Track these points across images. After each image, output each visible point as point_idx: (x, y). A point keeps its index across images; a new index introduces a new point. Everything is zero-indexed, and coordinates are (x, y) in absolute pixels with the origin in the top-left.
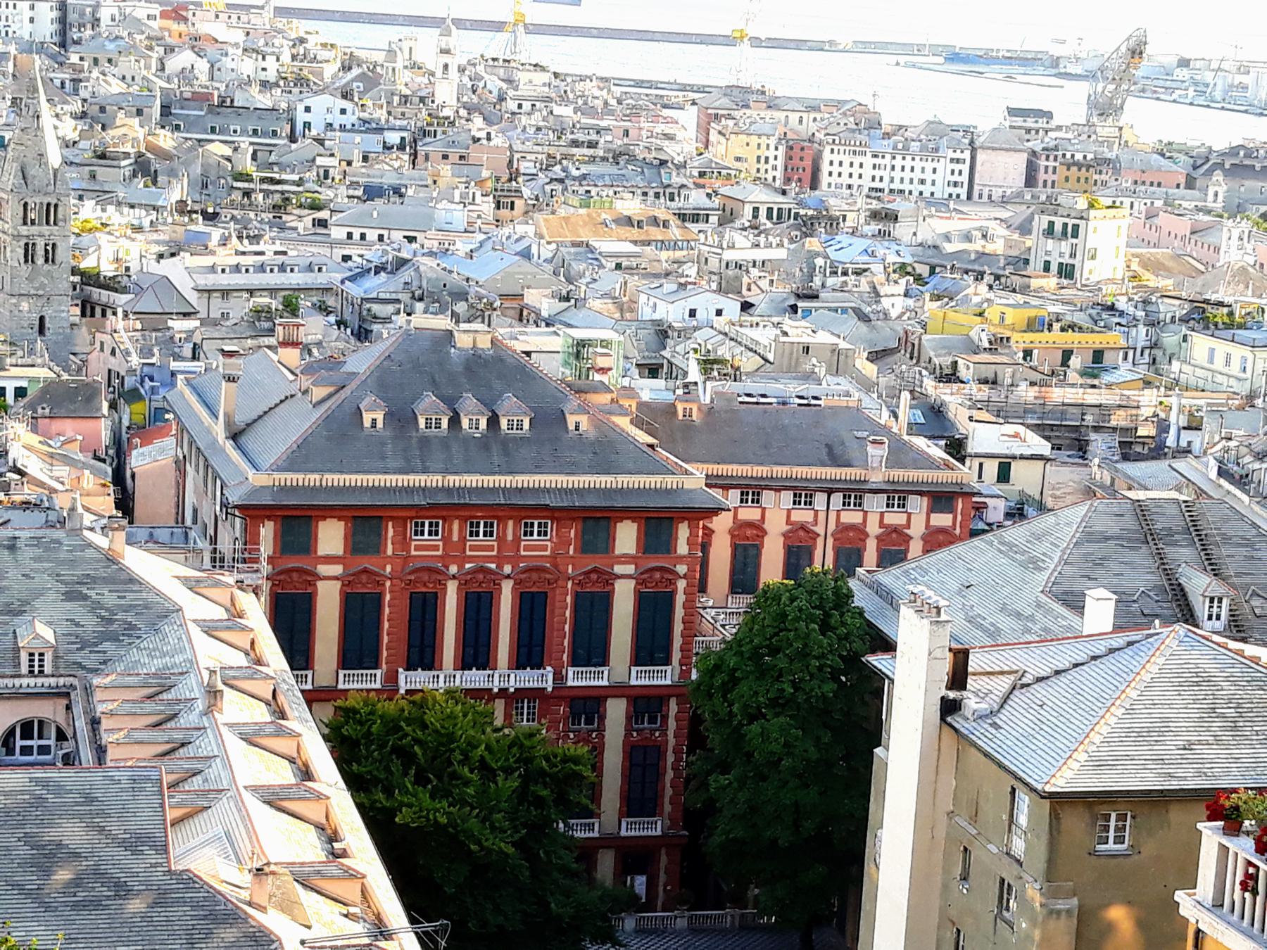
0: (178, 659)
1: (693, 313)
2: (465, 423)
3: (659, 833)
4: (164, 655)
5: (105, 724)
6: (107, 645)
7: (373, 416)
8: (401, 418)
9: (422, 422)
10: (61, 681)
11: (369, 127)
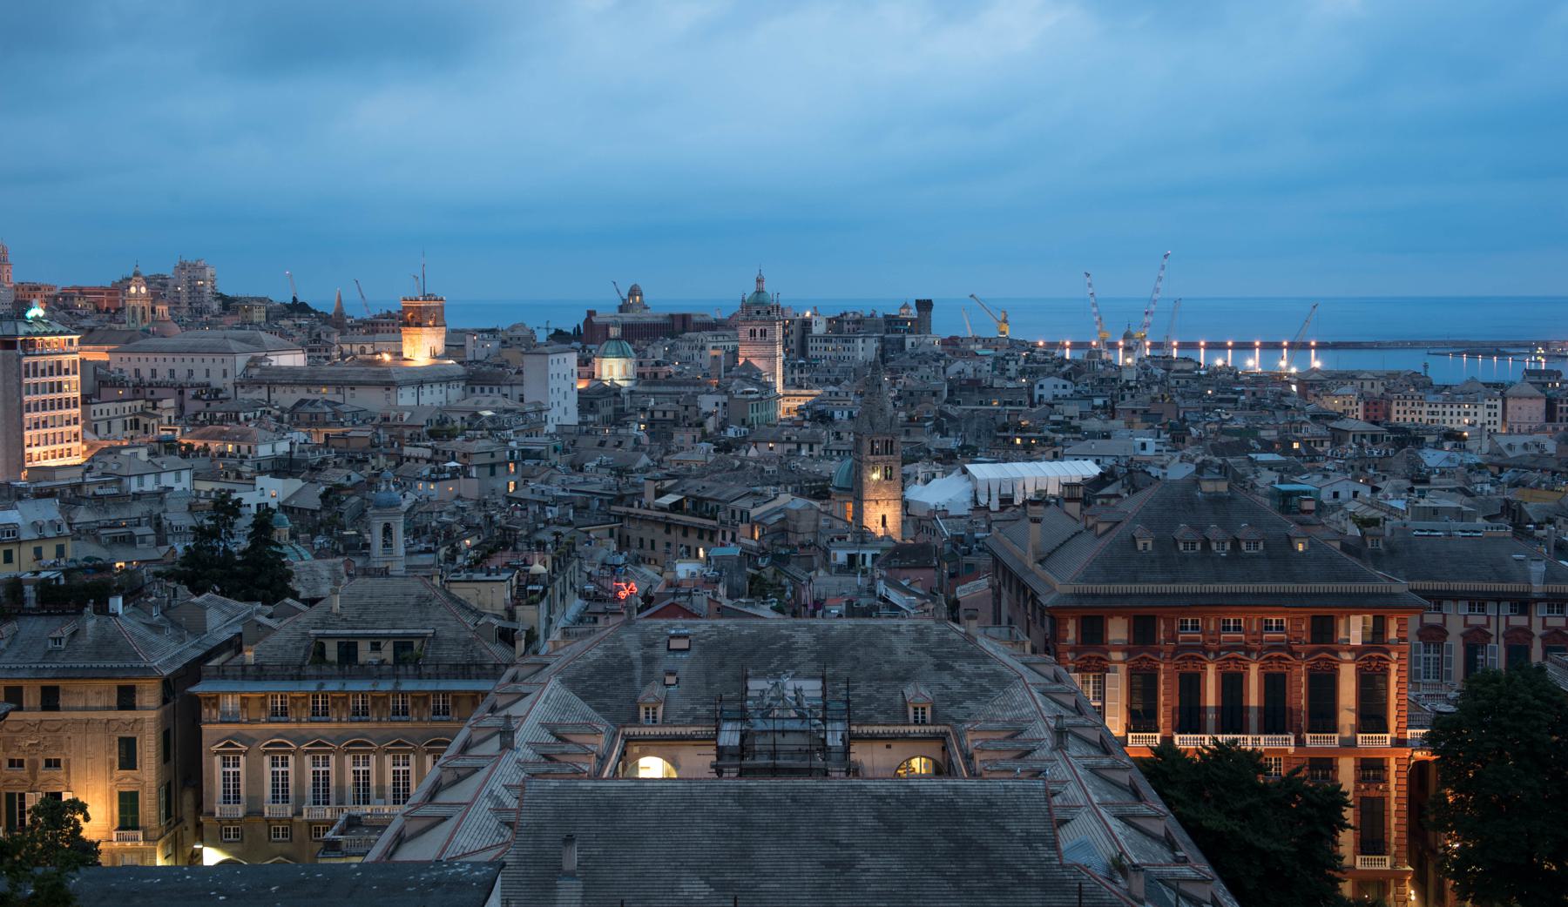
0: (1025, 711)
1: (1336, 495)
2: (1214, 546)
3: (1388, 867)
4: (1014, 709)
5: (978, 757)
6: (968, 703)
7: (1145, 543)
8: (1166, 545)
9: (1181, 547)
10: (938, 728)
11: (1079, 396)
